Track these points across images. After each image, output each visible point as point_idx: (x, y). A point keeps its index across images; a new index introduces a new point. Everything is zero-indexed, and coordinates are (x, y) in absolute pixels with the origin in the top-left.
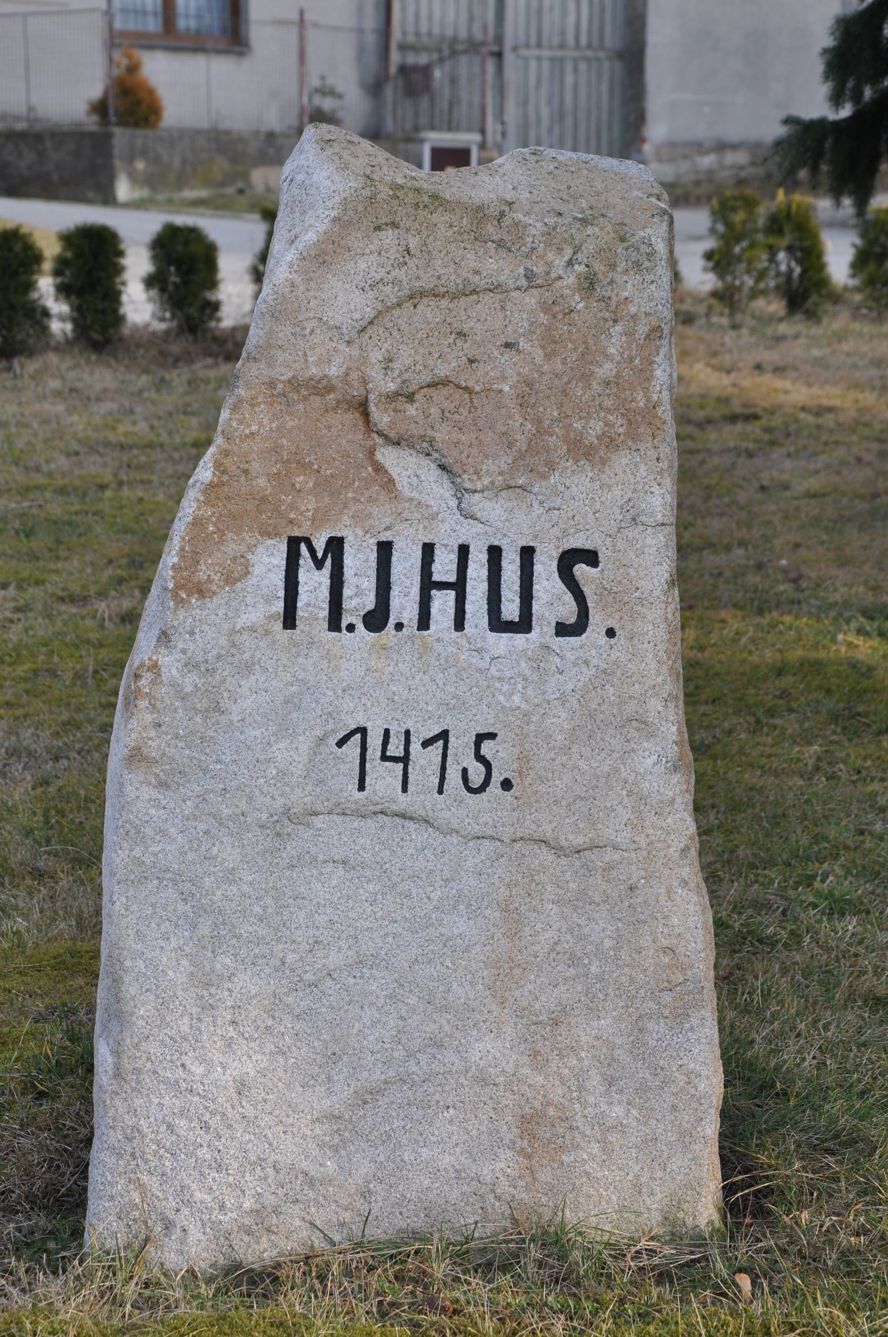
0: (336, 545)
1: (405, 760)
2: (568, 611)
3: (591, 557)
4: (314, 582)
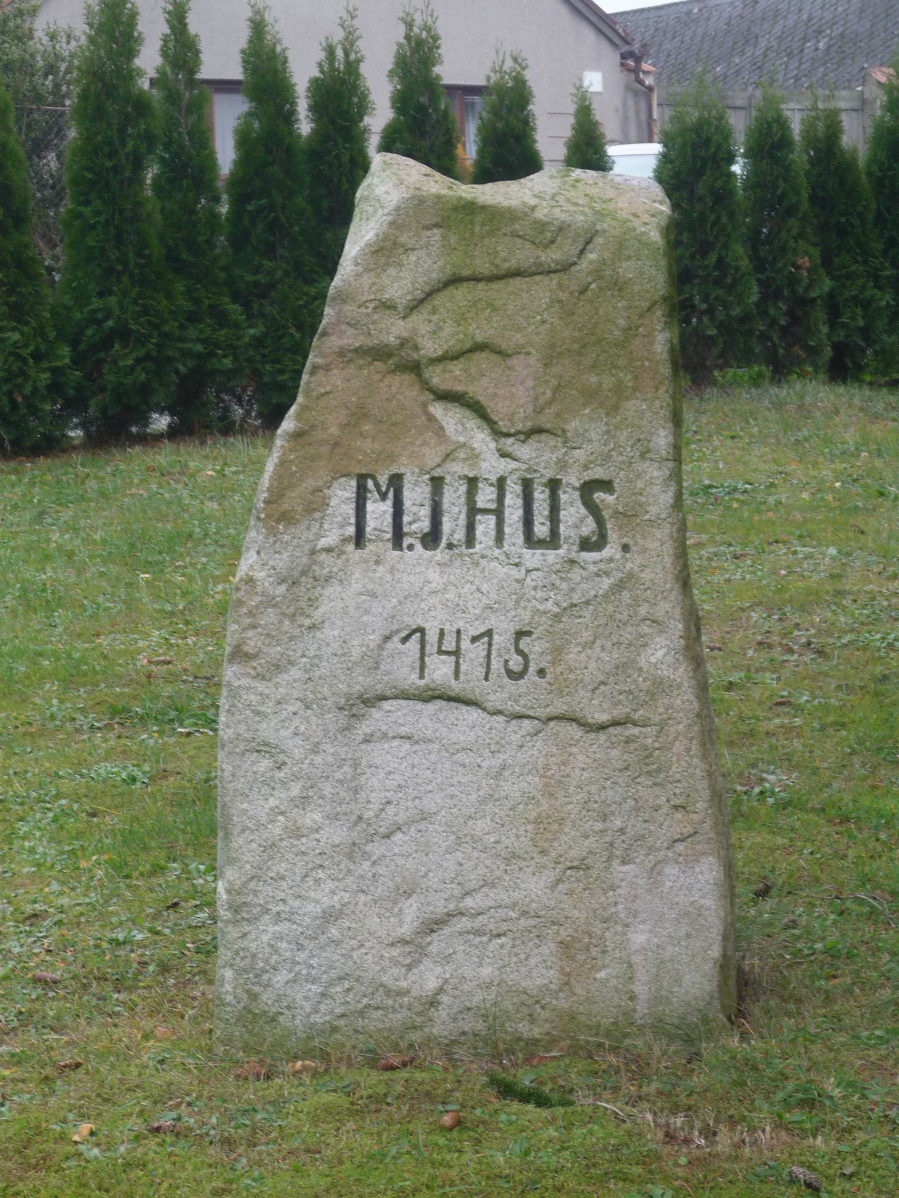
0: (396, 481)
1: (457, 653)
2: (589, 527)
3: (606, 485)
4: (378, 512)
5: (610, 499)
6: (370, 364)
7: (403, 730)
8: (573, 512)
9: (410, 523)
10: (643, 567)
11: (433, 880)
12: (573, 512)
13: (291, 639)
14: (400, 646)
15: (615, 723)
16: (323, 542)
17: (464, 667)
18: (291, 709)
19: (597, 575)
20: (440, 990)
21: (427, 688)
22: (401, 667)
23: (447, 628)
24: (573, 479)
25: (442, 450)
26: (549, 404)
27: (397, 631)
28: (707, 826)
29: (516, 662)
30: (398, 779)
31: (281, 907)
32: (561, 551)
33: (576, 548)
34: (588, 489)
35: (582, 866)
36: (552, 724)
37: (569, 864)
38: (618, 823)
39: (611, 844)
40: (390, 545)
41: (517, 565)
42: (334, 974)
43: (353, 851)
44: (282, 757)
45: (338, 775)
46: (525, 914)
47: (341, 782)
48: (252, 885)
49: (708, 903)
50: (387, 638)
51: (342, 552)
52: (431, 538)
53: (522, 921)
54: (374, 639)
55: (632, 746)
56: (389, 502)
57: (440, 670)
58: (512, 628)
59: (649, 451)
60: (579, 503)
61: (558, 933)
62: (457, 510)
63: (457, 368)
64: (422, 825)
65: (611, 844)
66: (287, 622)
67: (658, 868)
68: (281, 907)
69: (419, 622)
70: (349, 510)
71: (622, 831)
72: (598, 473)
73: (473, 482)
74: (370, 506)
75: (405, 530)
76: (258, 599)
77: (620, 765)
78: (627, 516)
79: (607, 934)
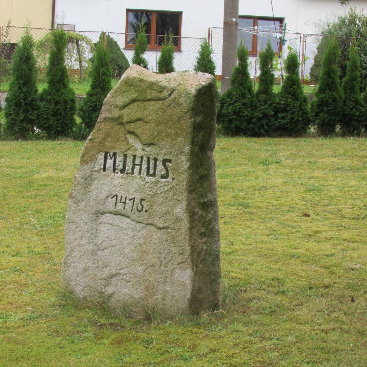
0: (115, 154)
1: (125, 203)
2: (164, 172)
3: (170, 161)
4: (110, 162)
5: (170, 164)
6: (112, 122)
7: (110, 222)
8: (160, 167)
9: (118, 166)
10: (177, 185)
11: (113, 263)
12: (160, 167)
13: (83, 194)
14: (111, 199)
15: (164, 228)
16: (95, 169)
17: (126, 207)
18: (81, 212)
19: (164, 185)
20: (113, 294)
21: (116, 211)
22: (110, 204)
23: (123, 195)
24: (160, 158)
25: (126, 147)
26: (156, 137)
27: (111, 195)
28: (189, 260)
29: (140, 207)
30: (107, 235)
31: (74, 265)
32: (156, 178)
33: (160, 177)
34: (165, 161)
35: (153, 266)
36: (148, 226)
37: (149, 265)
38: (164, 256)
39: (161, 261)
40: (112, 172)
41: (144, 180)
42: (86, 285)
43: (93, 253)
44: (78, 225)
45: (91, 232)
46: (136, 277)
47: (92, 234)
48: (68, 258)
49: (188, 282)
50: (108, 197)
51: (99, 172)
52: (123, 171)
53: (135, 279)
54: (104, 196)
55: (169, 235)
56: (113, 160)
57: (120, 207)
58: (140, 198)
59: (183, 152)
60: (162, 165)
61: (145, 284)
62: (130, 164)
63: (133, 125)
64: (112, 248)
65: (161, 261)
66: (83, 189)
67: (174, 270)
68: (74, 265)
69: (117, 193)
70: (102, 161)
71: (165, 258)
72: (168, 157)
73: (135, 157)
74: (108, 161)
75: (116, 168)
76: (76, 182)
77: (165, 239)
78: (175, 170)
79: (158, 286)
